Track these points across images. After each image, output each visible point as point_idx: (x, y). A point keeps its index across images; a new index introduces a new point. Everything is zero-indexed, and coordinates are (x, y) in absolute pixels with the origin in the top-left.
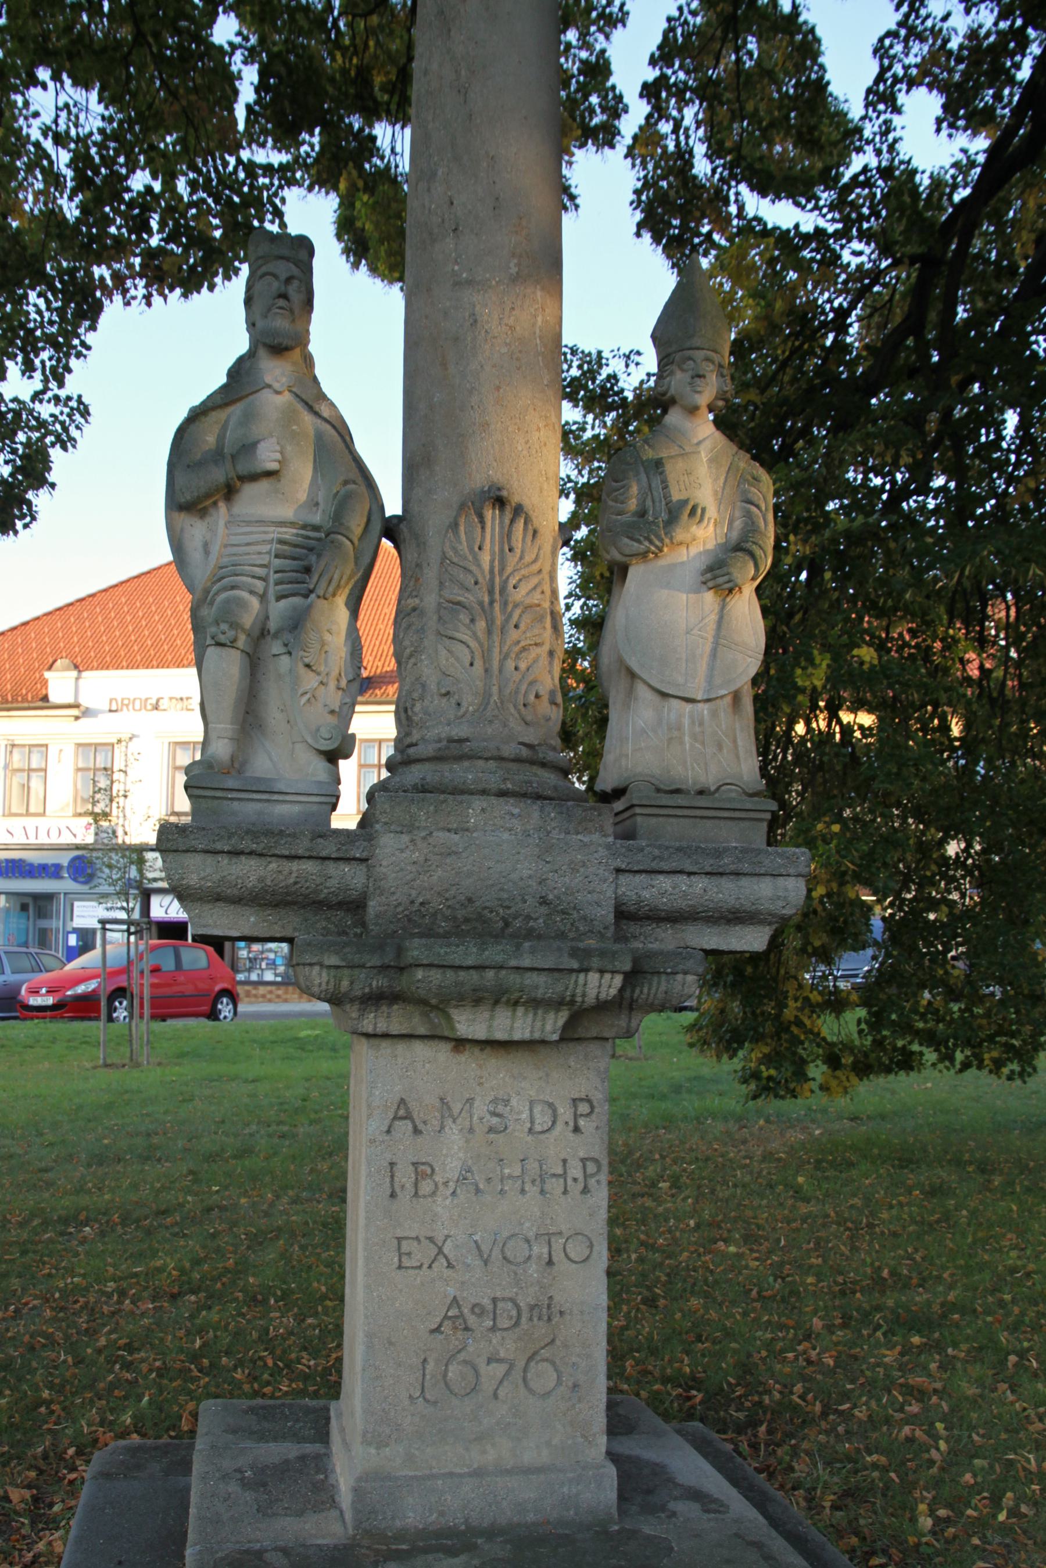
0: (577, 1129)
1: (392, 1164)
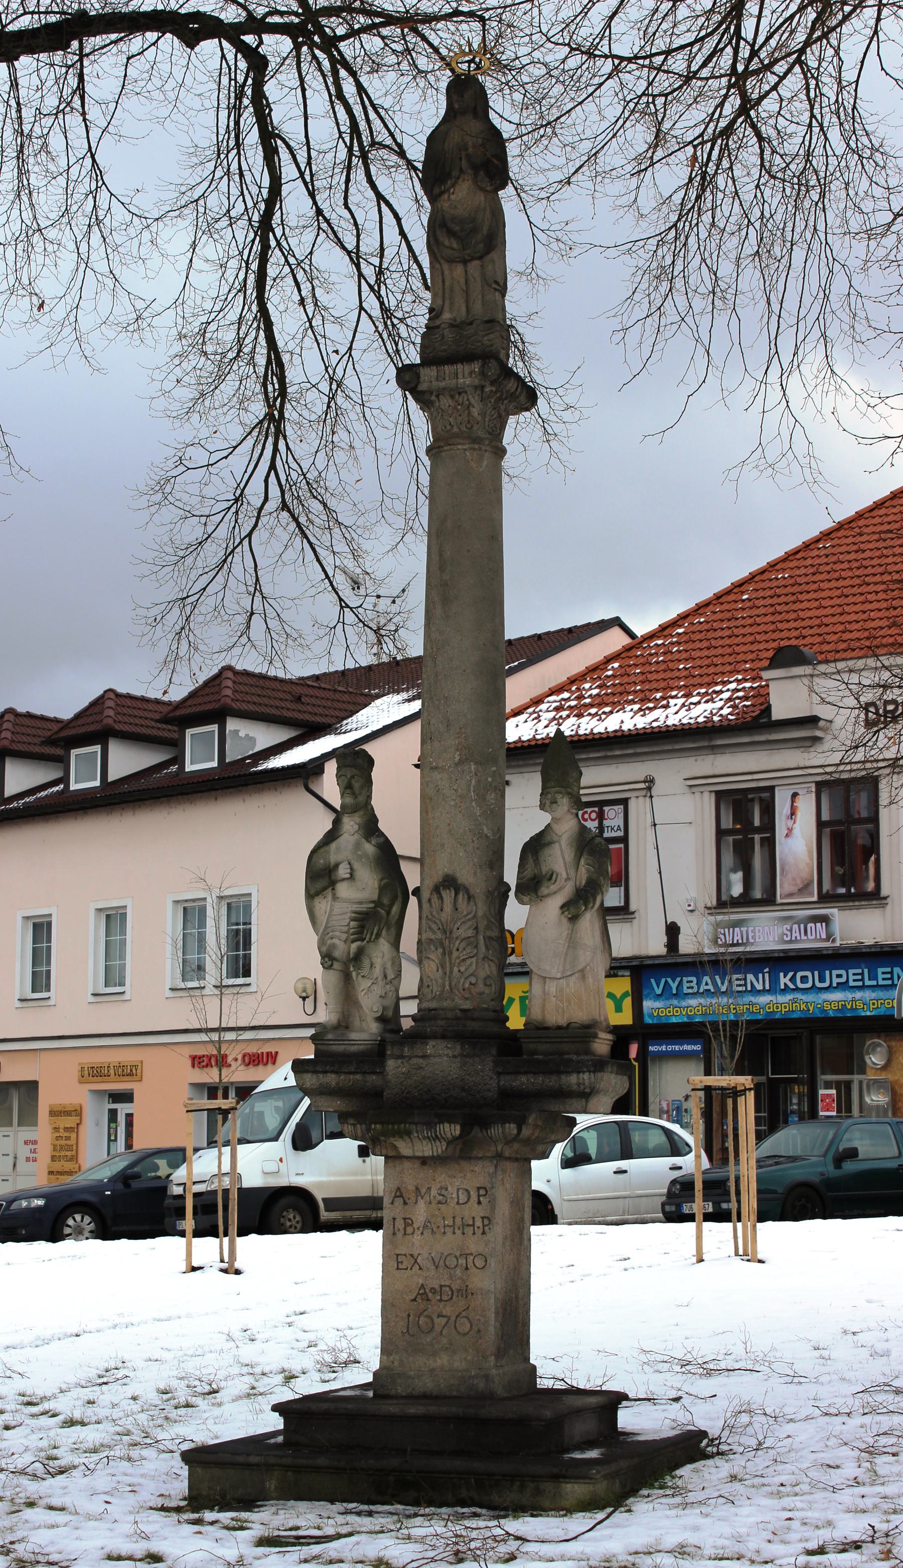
0: (479, 1203)
1: (394, 1219)
